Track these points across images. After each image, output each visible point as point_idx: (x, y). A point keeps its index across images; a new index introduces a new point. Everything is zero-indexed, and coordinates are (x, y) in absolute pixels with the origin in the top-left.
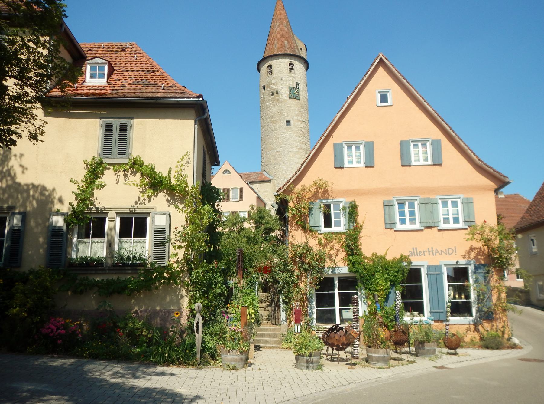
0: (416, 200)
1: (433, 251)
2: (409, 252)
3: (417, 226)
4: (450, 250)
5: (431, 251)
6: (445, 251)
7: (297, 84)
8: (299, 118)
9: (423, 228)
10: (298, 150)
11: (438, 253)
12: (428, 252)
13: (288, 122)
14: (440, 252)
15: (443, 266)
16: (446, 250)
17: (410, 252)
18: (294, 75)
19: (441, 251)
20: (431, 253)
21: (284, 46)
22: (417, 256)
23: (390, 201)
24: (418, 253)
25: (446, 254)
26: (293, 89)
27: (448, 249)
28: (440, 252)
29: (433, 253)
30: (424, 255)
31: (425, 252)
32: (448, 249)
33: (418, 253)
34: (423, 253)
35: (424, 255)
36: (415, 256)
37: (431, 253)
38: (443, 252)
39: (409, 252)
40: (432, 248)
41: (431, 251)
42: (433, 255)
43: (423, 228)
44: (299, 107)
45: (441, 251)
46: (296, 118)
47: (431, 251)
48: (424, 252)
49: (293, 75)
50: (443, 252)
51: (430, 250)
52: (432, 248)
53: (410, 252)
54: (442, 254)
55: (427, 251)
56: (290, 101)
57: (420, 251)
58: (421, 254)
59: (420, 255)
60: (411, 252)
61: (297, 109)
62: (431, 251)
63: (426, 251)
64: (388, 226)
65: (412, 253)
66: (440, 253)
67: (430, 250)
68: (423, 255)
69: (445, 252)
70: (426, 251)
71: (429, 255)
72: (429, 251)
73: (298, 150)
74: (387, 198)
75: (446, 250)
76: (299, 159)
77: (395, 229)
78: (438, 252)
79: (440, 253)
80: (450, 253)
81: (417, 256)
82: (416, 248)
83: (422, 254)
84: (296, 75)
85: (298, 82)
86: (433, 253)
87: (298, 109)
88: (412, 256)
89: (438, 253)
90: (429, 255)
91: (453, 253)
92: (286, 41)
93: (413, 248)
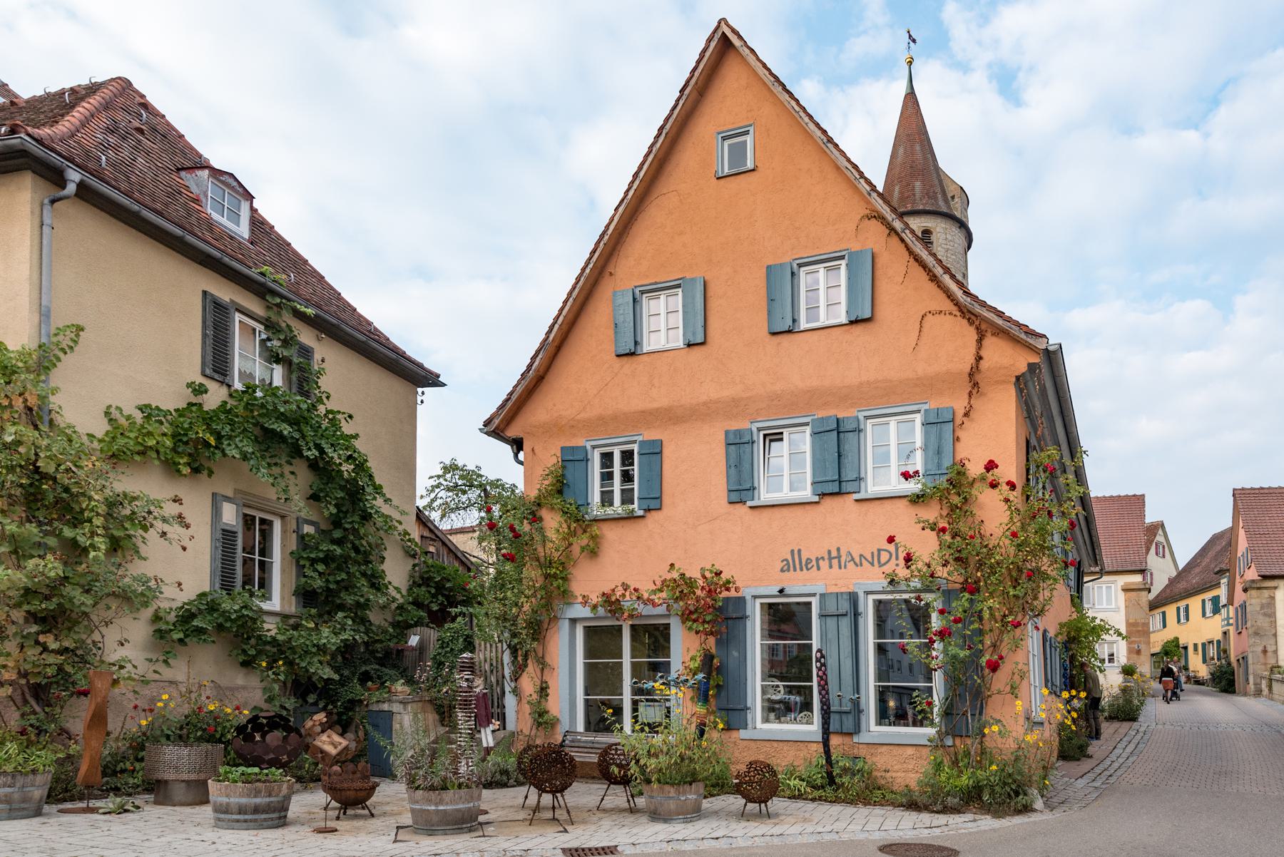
0: (807, 424)
1: (839, 557)
2: (782, 561)
3: (806, 493)
4: (882, 552)
5: (835, 558)
6: (870, 555)
9: (816, 499)
11: (852, 562)
12: (827, 561)
14: (857, 560)
15: (861, 595)
16: (873, 553)
17: (785, 562)
19: (861, 555)
20: (835, 562)
21: (914, 195)
22: (802, 570)
23: (739, 433)
24: (804, 563)
25: (872, 564)
27: (879, 550)
28: (857, 560)
29: (839, 562)
30: (819, 568)
31: (821, 562)
32: (879, 550)
33: (804, 563)
34: (814, 563)
35: (819, 568)
36: (795, 570)
37: (835, 562)
38: (866, 559)
39: (782, 561)
40: (838, 550)
41: (834, 558)
42: (840, 568)
43: (816, 499)
45: (861, 555)
47: (834, 558)
48: (817, 559)
50: (866, 559)
51: (834, 554)
52: (838, 550)
53: (785, 562)
54: (861, 565)
55: (826, 557)
57: (808, 559)
58: (809, 566)
59: (808, 569)
60: (786, 560)
62: (835, 558)
63: (823, 558)
64: (735, 497)
65: (788, 564)
66: (859, 563)
67: (834, 554)
68: (815, 568)
69: (870, 559)
70: (823, 558)
71: (831, 567)
72: (830, 559)
74: (735, 425)
75: (873, 553)
77: (749, 503)
78: (853, 559)
79: (859, 563)
80: (883, 560)
81: (802, 570)
82: (799, 551)
83: (813, 566)
86: (839, 562)
88: (788, 570)
89: (852, 562)
90: (831, 567)
91: (892, 561)
92: (918, 184)
93: (792, 551)
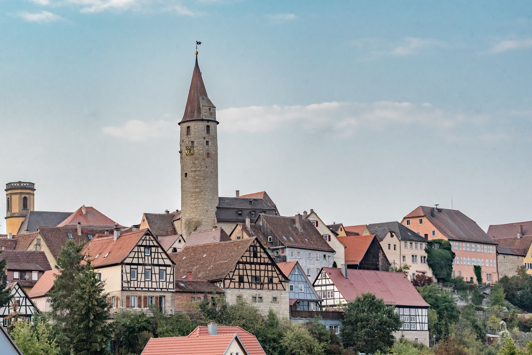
7: (192, 142)
8: (193, 169)
10: (191, 194)
13: (186, 174)
18: (190, 136)
26: (188, 147)
44: (193, 161)
46: (190, 170)
49: (189, 136)
56: (187, 158)
61: (191, 163)
73: (191, 194)
76: (192, 201)
84: (191, 136)
85: (193, 140)
87: (192, 162)
